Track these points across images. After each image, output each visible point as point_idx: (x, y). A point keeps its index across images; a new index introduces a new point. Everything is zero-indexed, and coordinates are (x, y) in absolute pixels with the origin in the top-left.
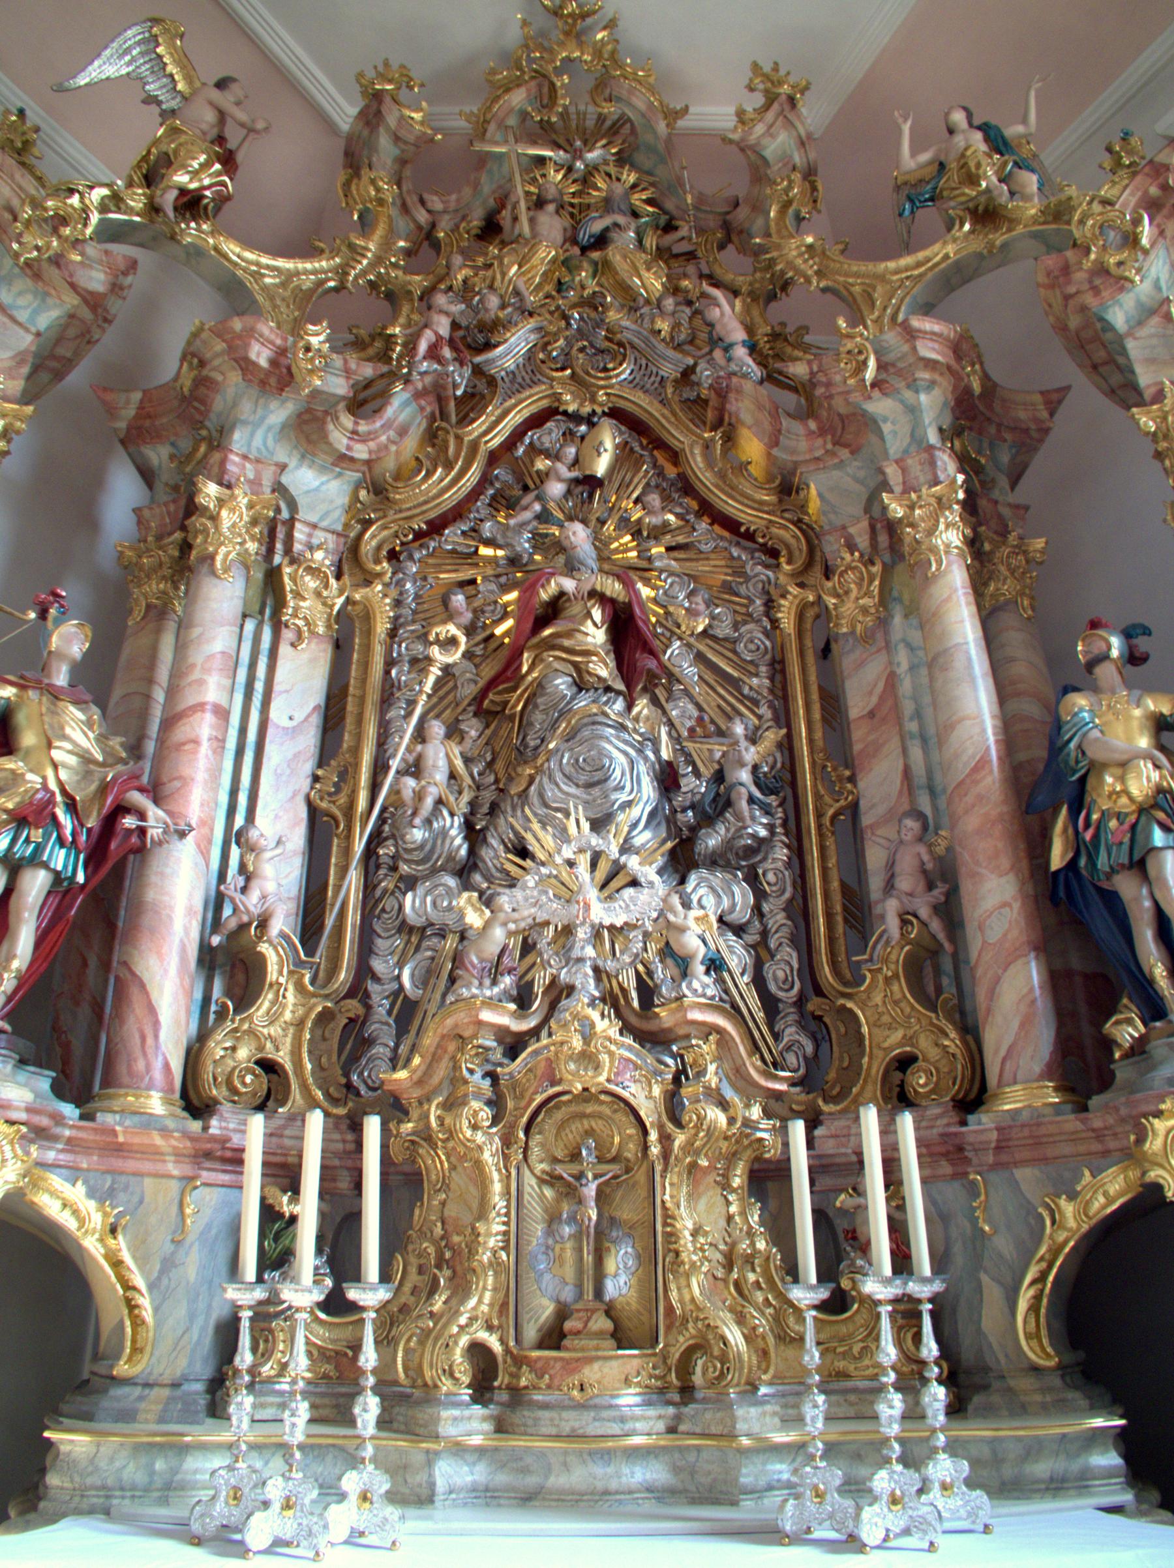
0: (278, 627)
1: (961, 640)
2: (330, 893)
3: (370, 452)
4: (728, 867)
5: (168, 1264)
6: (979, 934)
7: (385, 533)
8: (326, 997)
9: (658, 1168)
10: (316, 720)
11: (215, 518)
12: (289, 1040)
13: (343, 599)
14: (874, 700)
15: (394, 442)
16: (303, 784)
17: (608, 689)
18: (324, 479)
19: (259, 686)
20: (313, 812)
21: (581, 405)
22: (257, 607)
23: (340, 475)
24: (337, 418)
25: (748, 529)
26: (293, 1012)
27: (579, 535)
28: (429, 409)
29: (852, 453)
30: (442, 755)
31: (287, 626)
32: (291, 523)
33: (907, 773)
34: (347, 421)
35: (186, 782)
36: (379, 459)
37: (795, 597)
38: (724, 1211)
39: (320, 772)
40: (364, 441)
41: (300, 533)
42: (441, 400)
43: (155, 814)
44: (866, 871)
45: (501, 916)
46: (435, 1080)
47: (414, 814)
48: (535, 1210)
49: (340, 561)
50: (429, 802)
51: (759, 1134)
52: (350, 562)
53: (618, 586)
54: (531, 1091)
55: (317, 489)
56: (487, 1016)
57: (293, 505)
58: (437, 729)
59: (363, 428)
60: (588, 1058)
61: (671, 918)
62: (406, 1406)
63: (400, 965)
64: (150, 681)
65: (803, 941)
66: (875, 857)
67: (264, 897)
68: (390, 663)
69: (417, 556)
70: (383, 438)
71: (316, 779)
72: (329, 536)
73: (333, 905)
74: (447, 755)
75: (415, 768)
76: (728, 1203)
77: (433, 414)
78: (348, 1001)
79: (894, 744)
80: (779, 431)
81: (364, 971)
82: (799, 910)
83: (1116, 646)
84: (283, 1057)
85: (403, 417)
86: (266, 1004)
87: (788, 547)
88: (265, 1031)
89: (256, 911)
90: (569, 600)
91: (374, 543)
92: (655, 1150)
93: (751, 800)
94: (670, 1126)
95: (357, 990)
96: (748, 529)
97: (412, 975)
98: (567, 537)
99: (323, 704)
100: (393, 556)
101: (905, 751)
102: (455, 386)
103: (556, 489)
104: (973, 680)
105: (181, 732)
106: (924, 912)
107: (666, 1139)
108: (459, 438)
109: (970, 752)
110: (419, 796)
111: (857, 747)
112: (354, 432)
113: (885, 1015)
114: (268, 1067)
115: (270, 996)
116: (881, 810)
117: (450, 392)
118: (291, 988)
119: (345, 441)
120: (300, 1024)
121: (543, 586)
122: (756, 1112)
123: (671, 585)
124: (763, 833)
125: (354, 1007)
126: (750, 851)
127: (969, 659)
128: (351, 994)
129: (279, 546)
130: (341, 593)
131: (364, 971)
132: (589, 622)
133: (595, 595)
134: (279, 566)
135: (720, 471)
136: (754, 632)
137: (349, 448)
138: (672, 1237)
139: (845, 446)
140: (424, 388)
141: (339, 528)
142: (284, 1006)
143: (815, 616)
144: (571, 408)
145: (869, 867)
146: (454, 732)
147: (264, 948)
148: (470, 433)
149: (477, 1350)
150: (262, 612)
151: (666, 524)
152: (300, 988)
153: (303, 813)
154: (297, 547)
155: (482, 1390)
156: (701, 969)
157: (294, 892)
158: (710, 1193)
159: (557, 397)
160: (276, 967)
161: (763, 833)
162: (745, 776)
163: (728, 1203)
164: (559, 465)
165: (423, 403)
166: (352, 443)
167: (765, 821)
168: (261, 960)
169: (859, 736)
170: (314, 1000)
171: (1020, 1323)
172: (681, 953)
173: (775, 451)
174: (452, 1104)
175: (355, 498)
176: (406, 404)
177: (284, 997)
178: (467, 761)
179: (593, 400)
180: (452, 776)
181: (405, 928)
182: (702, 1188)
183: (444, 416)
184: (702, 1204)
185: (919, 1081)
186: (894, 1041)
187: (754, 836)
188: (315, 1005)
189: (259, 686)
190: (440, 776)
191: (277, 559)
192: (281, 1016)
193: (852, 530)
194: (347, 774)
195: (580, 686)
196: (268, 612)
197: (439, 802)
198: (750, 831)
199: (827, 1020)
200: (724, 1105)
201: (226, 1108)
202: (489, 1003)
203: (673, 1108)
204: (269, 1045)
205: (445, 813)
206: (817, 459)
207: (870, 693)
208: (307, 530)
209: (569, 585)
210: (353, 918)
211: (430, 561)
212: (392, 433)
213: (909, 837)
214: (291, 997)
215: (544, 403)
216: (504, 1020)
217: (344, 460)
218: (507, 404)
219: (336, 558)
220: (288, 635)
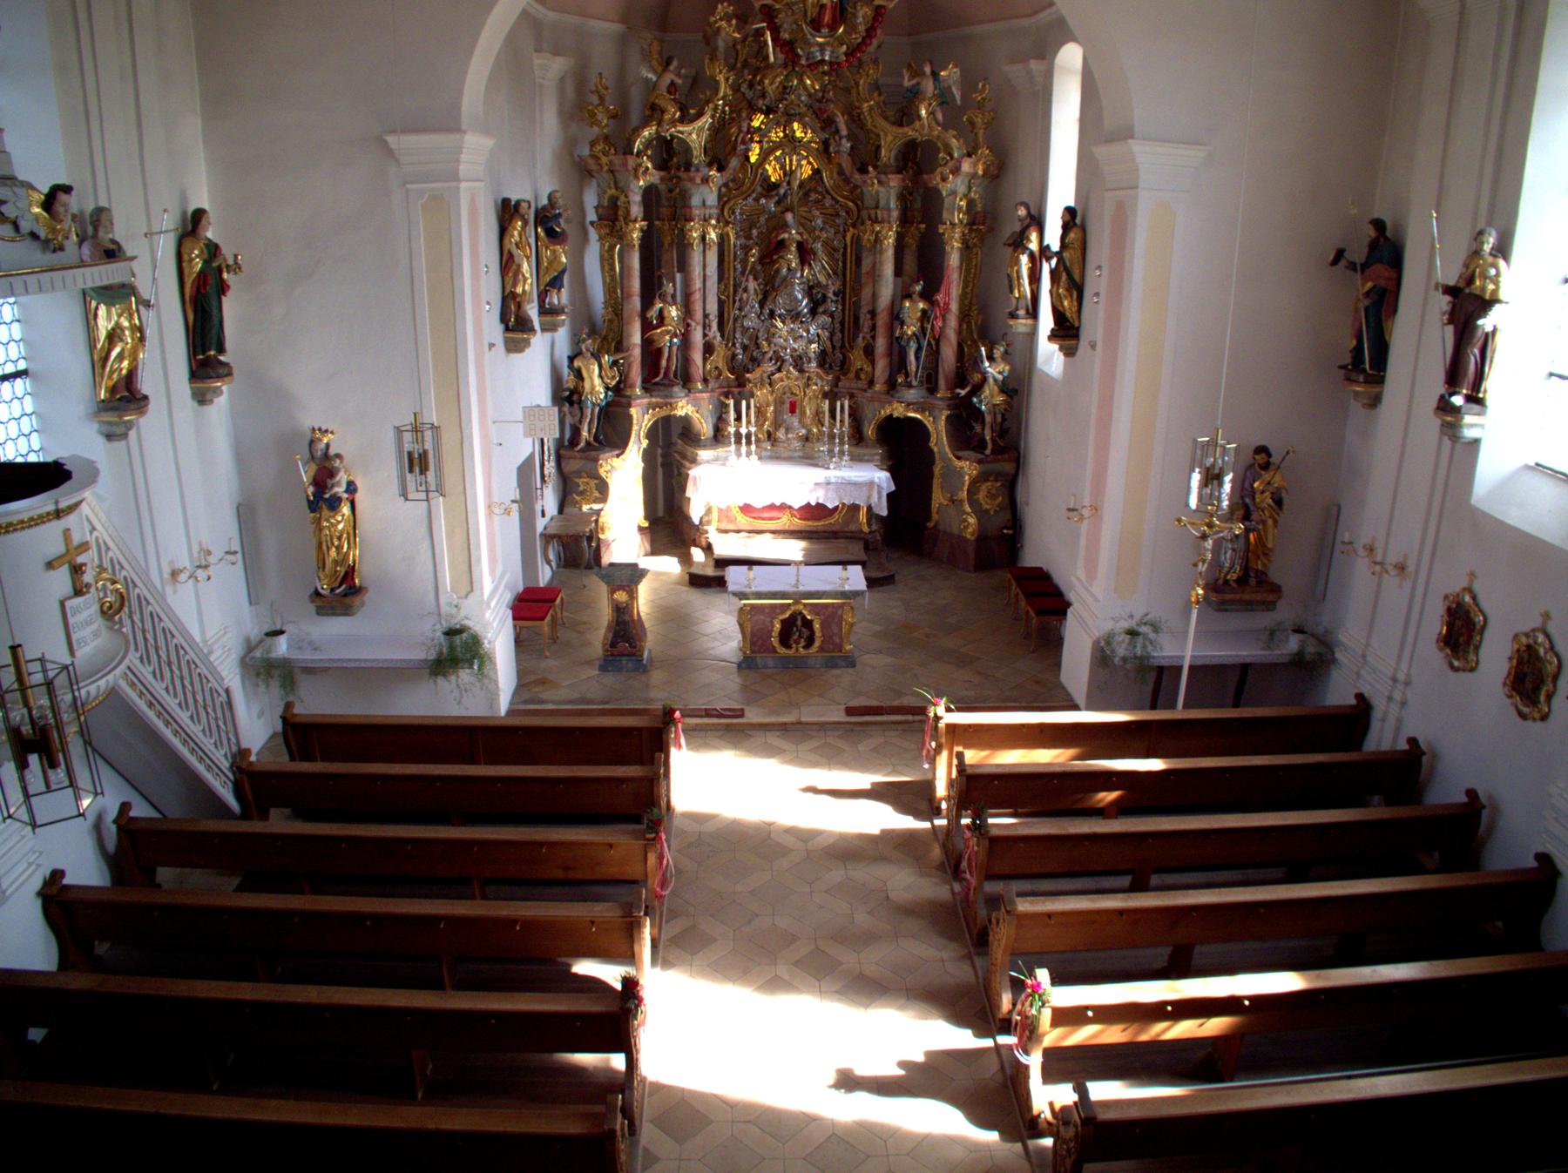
65: (842, 331)
75: (745, 290)
82: (842, 323)
83: (918, 288)
84: (720, 365)
113: (857, 360)
136: (840, 236)
143: (857, 241)
146: (756, 279)
169: (864, 280)
171: (870, 431)
185: (862, 376)
186: (858, 365)
192: (719, 359)
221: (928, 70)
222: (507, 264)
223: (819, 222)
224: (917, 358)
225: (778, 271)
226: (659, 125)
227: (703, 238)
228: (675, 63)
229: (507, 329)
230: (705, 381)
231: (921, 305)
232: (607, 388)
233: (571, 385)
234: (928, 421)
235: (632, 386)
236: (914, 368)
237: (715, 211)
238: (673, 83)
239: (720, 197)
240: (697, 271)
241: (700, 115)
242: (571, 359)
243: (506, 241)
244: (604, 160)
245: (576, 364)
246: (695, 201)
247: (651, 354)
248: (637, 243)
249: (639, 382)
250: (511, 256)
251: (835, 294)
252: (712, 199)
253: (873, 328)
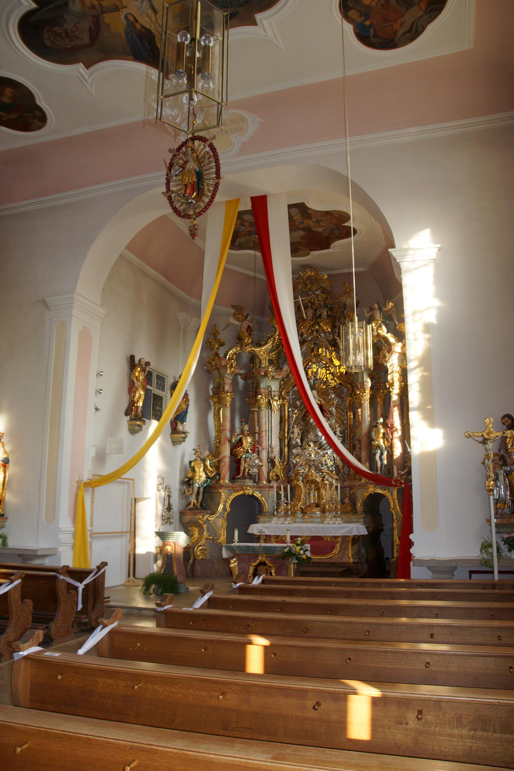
0: (271, 410)
5: (268, 500)
10: (279, 424)
11: (260, 400)
16: (278, 434)
19: (270, 420)
20: (280, 439)
32: (271, 392)
35: (263, 442)
41: (273, 393)
43: (260, 448)
48: (307, 492)
52: (281, 397)
58: (295, 426)
60: (312, 475)
62: (294, 514)
64: (255, 422)
68: (289, 412)
81: (288, 461)
84: (279, 474)
95: (288, 463)
105: (261, 435)
110: (293, 437)
114: (277, 475)
120: (281, 469)
131: (288, 461)
138: (322, 495)
141: (278, 390)
149: (301, 508)
153: (278, 439)
178: (300, 430)
190: (296, 434)
200: (328, 480)
201: (272, 481)
203: (323, 480)
214: (279, 466)
220: (273, 412)
221: (376, 306)
222: (132, 388)
223: (333, 396)
224: (381, 460)
225: (308, 421)
226: (241, 347)
227: (269, 404)
228: (249, 317)
229: (131, 420)
230: (269, 481)
231: (382, 431)
232: (208, 477)
233: (190, 475)
234: (388, 495)
235: (224, 479)
236: (379, 465)
237: (277, 393)
238: (249, 327)
239: (280, 386)
240: (264, 420)
241: (266, 343)
242: (190, 462)
243: (132, 376)
244: (213, 363)
245: (193, 464)
246: (262, 385)
247: (236, 462)
248: (228, 405)
249: (227, 477)
250: (134, 383)
251: (341, 433)
252: (275, 386)
253: (360, 449)
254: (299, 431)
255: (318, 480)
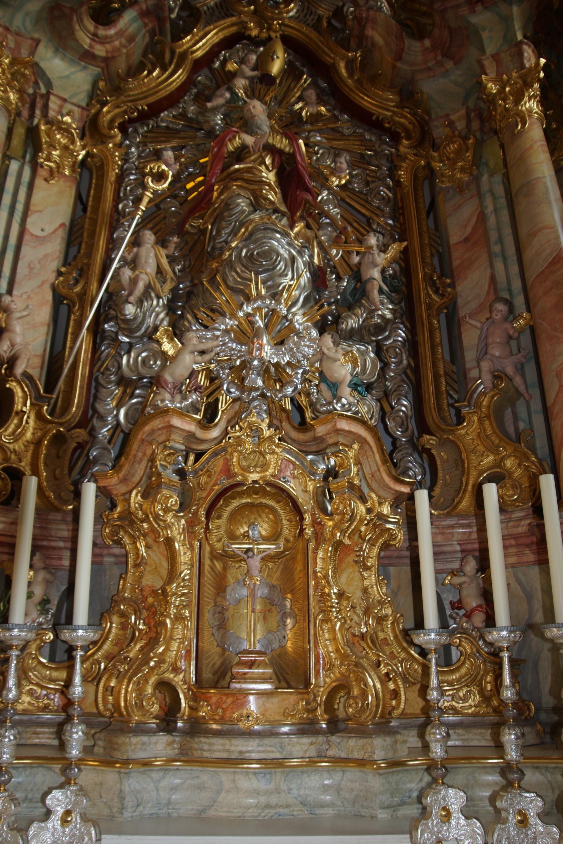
0: (35, 166)
1: (541, 175)
2: (67, 354)
3: (107, 52)
4: (362, 341)
6: (556, 380)
7: (117, 111)
8: (61, 424)
9: (312, 545)
10: (62, 234)
12: (29, 454)
13: (84, 152)
14: (469, 230)
15: (125, 47)
16: (51, 277)
17: (276, 211)
18: (73, 70)
19: (20, 207)
21: (261, 31)
22: (21, 154)
23: (85, 68)
24: (82, 20)
25: (378, 117)
26: (33, 434)
27: (258, 108)
28: (150, 25)
29: (455, 64)
30: (152, 255)
31: (42, 167)
32: (46, 97)
33: (493, 279)
34: (90, 25)
36: (113, 58)
37: (412, 161)
38: (360, 584)
39: (63, 269)
40: (102, 43)
41: (54, 103)
42: (161, 20)
44: (462, 348)
45: (190, 348)
46: (136, 479)
47: (130, 294)
49: (84, 128)
50: (141, 285)
51: (388, 526)
52: (92, 129)
53: (285, 142)
54: (211, 484)
55: (68, 77)
56: (177, 422)
57: (49, 84)
59: (102, 32)
61: (326, 351)
63: (118, 407)
66: (470, 337)
67: (13, 345)
68: (117, 199)
69: (141, 131)
70: (117, 43)
71: (60, 274)
72: (76, 109)
73: (67, 361)
74: (156, 255)
76: (363, 578)
77: (154, 29)
78: (78, 430)
79: (484, 258)
80: (403, 50)
85: (131, 30)
86: (13, 426)
87: (406, 130)
88: (11, 446)
89: (6, 356)
90: (249, 152)
91: (109, 117)
92: (309, 531)
93: (381, 291)
94: (320, 516)
96: (378, 117)
97: (126, 415)
98: (249, 110)
99: (68, 223)
100: (123, 128)
101: (492, 265)
102: (171, 10)
103: (240, 84)
104: (549, 203)
106: (510, 370)
107: (316, 523)
108: (173, 53)
109: (548, 251)
110: (134, 282)
111: (456, 263)
112: (95, 35)
115: (16, 421)
116: (474, 305)
117: (167, 13)
118: (32, 416)
119: (88, 41)
120: (38, 443)
121: (230, 140)
122: (386, 510)
123: (322, 154)
124: (389, 315)
125: (81, 434)
126: (379, 329)
127: (547, 188)
128: (79, 425)
129: (38, 112)
130: (84, 147)
132: (263, 168)
133: (270, 149)
134: (38, 126)
135: (358, 79)
137: (91, 46)
139: (451, 58)
140: (147, 9)
141: (84, 104)
142: (25, 430)
144: (254, 33)
145: (464, 345)
146: (162, 242)
147: (12, 385)
148: (181, 46)
150: (24, 157)
151: (319, 114)
152: (40, 417)
153: (49, 296)
154: (51, 113)
155: (167, 721)
156: (348, 390)
157: (40, 352)
158: (350, 570)
159: (243, 25)
160: (21, 400)
161: (389, 315)
162: (376, 274)
163: (363, 578)
164: (244, 67)
165: (146, 21)
166: (93, 44)
167: (391, 307)
168: (10, 393)
169: (457, 257)
170: (50, 426)
172: (333, 380)
173: (399, 64)
174: (148, 493)
175: (95, 85)
176: (134, 20)
177: (27, 422)
178: (172, 260)
179: (269, 29)
180: (160, 271)
181: (123, 381)
182: (344, 566)
183: (162, 32)
184: (343, 579)
187: (382, 317)
188: (51, 430)
189: (20, 207)
191: (36, 121)
193: (453, 117)
194: (84, 273)
195: (256, 206)
196: (28, 157)
197: (149, 287)
198: (380, 313)
199: (433, 451)
202: (181, 413)
204: (13, 456)
205: (153, 295)
206: (429, 69)
207: (466, 226)
208: (59, 102)
209: (249, 140)
210: (82, 370)
211: (149, 135)
212: (123, 40)
213: (498, 317)
215: (234, 29)
216: (192, 428)
217: (87, 57)
218: (207, 29)
219: (81, 125)
220: (42, 173)
254: (164, 262)
255: (301, 488)
